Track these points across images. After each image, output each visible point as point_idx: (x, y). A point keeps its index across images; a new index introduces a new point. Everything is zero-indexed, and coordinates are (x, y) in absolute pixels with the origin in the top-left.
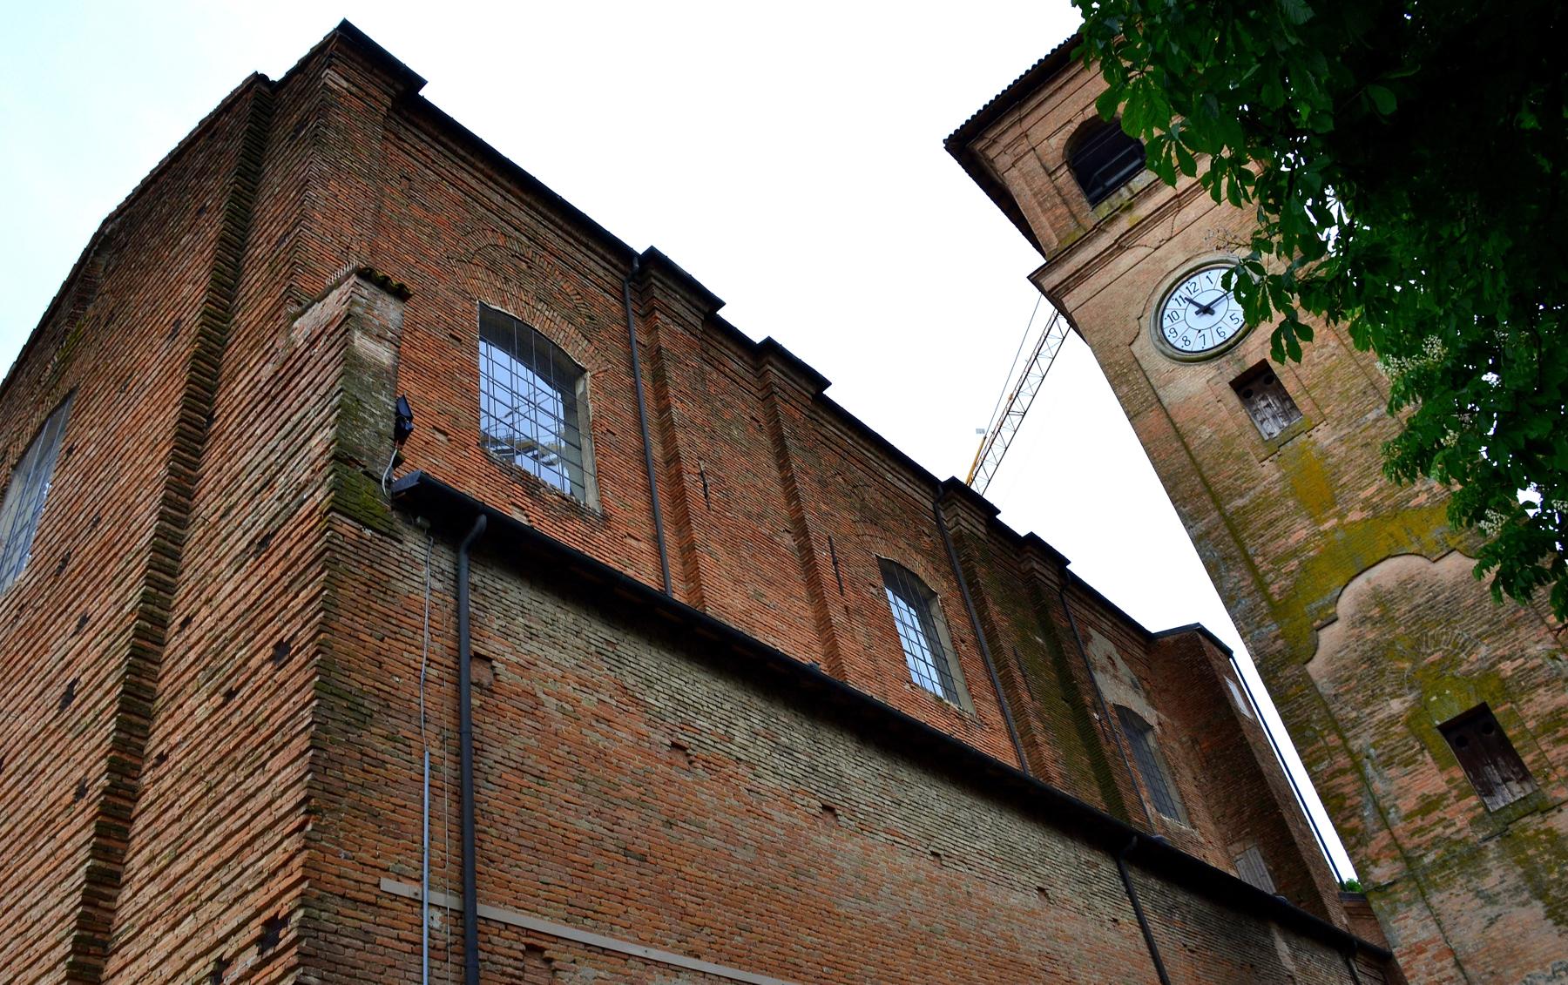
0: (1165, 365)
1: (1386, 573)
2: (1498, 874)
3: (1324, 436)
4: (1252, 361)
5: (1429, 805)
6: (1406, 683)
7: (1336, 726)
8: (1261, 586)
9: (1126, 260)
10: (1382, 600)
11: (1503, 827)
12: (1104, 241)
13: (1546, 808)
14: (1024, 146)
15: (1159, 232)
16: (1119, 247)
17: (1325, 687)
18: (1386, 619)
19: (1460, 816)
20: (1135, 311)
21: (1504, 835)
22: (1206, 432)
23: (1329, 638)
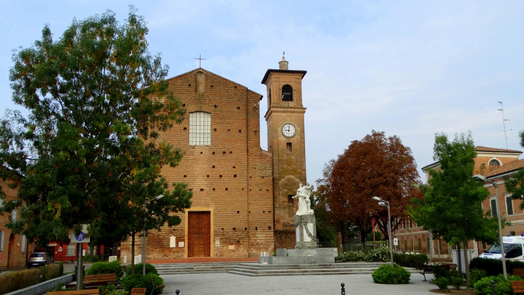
0: (281, 134)
1: (292, 177)
2: (287, 211)
3: (293, 157)
4: (290, 142)
5: (284, 202)
6: (287, 189)
7: (279, 189)
8: (279, 170)
9: (283, 114)
10: (289, 180)
11: (289, 207)
12: (282, 110)
13: (293, 207)
14: (278, 80)
15: (289, 114)
16: (283, 112)
17: (280, 185)
18: (289, 181)
19: (286, 204)
20: (281, 123)
21: (289, 208)
22: (281, 147)
23: (283, 180)
